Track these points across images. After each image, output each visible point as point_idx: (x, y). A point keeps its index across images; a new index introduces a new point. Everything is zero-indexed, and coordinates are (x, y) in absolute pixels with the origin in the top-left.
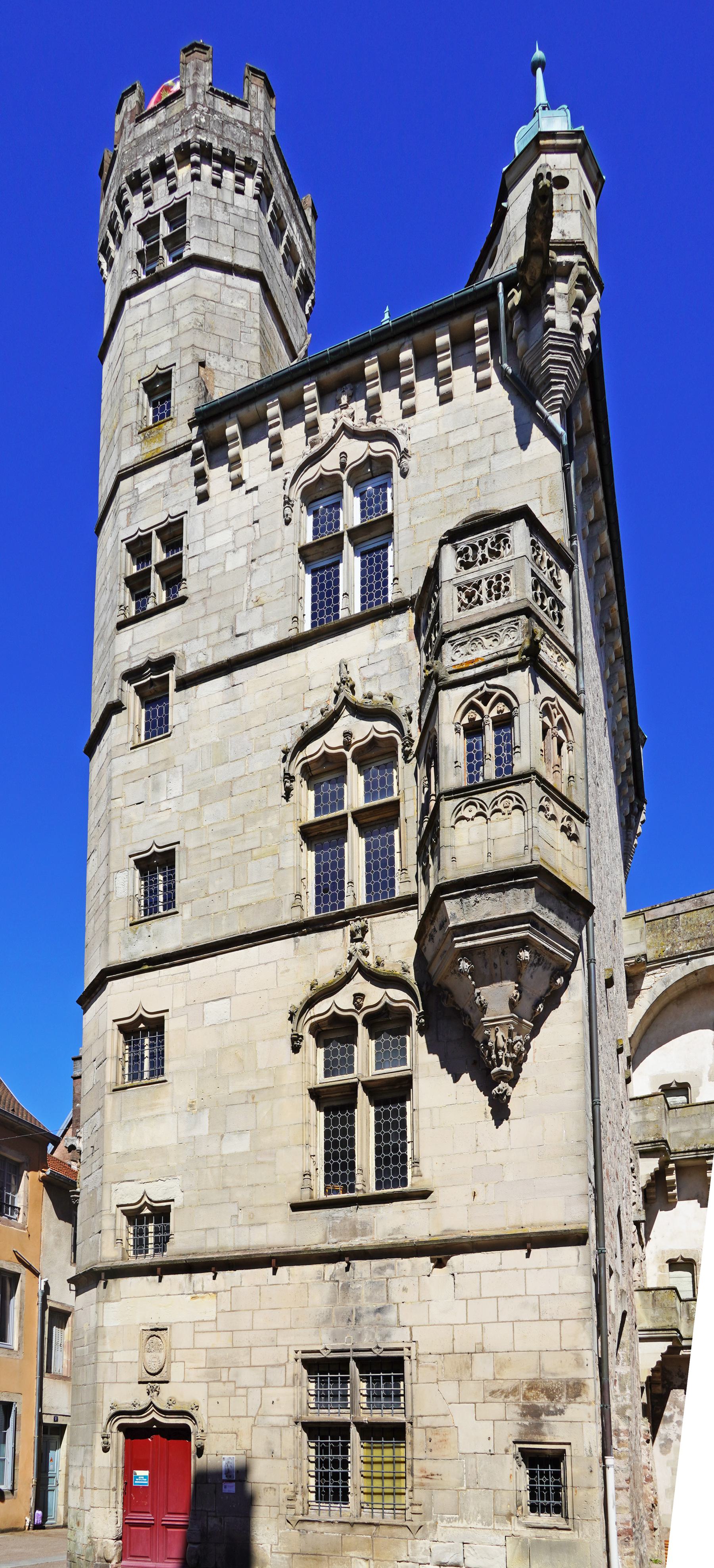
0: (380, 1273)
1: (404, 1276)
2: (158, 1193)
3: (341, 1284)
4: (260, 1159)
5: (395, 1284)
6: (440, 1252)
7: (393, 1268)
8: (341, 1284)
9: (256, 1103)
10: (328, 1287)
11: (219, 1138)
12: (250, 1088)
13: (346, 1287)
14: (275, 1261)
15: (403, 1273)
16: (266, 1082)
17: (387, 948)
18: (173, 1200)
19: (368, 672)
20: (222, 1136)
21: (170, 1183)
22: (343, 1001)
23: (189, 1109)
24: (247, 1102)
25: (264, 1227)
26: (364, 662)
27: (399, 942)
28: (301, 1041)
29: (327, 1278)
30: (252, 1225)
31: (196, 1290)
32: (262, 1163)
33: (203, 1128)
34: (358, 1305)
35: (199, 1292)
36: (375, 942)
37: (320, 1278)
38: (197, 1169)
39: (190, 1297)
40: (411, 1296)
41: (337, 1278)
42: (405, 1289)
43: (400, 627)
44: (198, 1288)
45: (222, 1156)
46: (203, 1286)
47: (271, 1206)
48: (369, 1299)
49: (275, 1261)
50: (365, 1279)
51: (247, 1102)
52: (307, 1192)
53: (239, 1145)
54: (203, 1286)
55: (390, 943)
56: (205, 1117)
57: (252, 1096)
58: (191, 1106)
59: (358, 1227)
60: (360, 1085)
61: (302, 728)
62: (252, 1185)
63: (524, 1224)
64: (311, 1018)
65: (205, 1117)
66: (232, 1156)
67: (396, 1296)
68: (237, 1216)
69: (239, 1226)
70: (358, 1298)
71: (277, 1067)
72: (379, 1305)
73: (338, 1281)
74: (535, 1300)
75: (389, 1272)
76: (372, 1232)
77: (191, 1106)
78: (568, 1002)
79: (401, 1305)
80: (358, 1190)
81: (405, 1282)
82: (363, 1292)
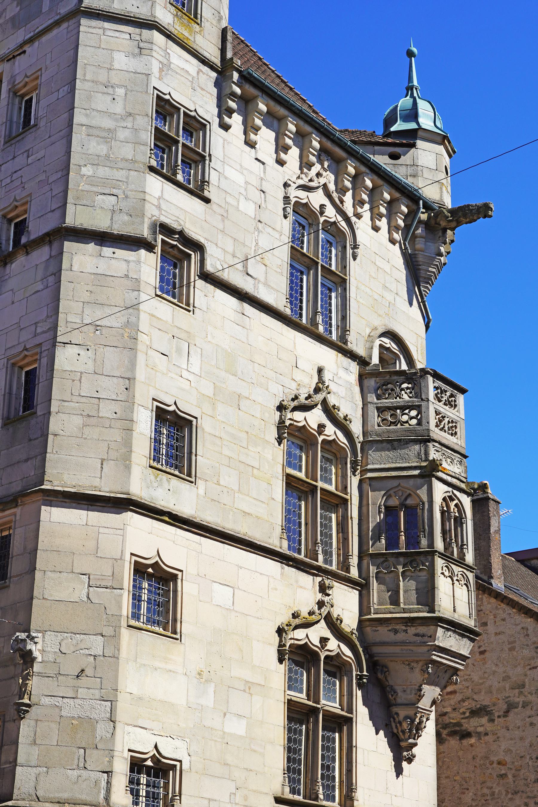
2: (170, 750)
11: (222, 715)
12: (247, 679)
20: (225, 714)
21: (178, 743)
23: (198, 677)
32: (255, 751)
33: (209, 700)
38: (203, 738)
43: (351, 369)
45: (224, 733)
47: (261, 793)
58: (199, 674)
62: (247, 769)
68: (235, 794)
71: (267, 669)
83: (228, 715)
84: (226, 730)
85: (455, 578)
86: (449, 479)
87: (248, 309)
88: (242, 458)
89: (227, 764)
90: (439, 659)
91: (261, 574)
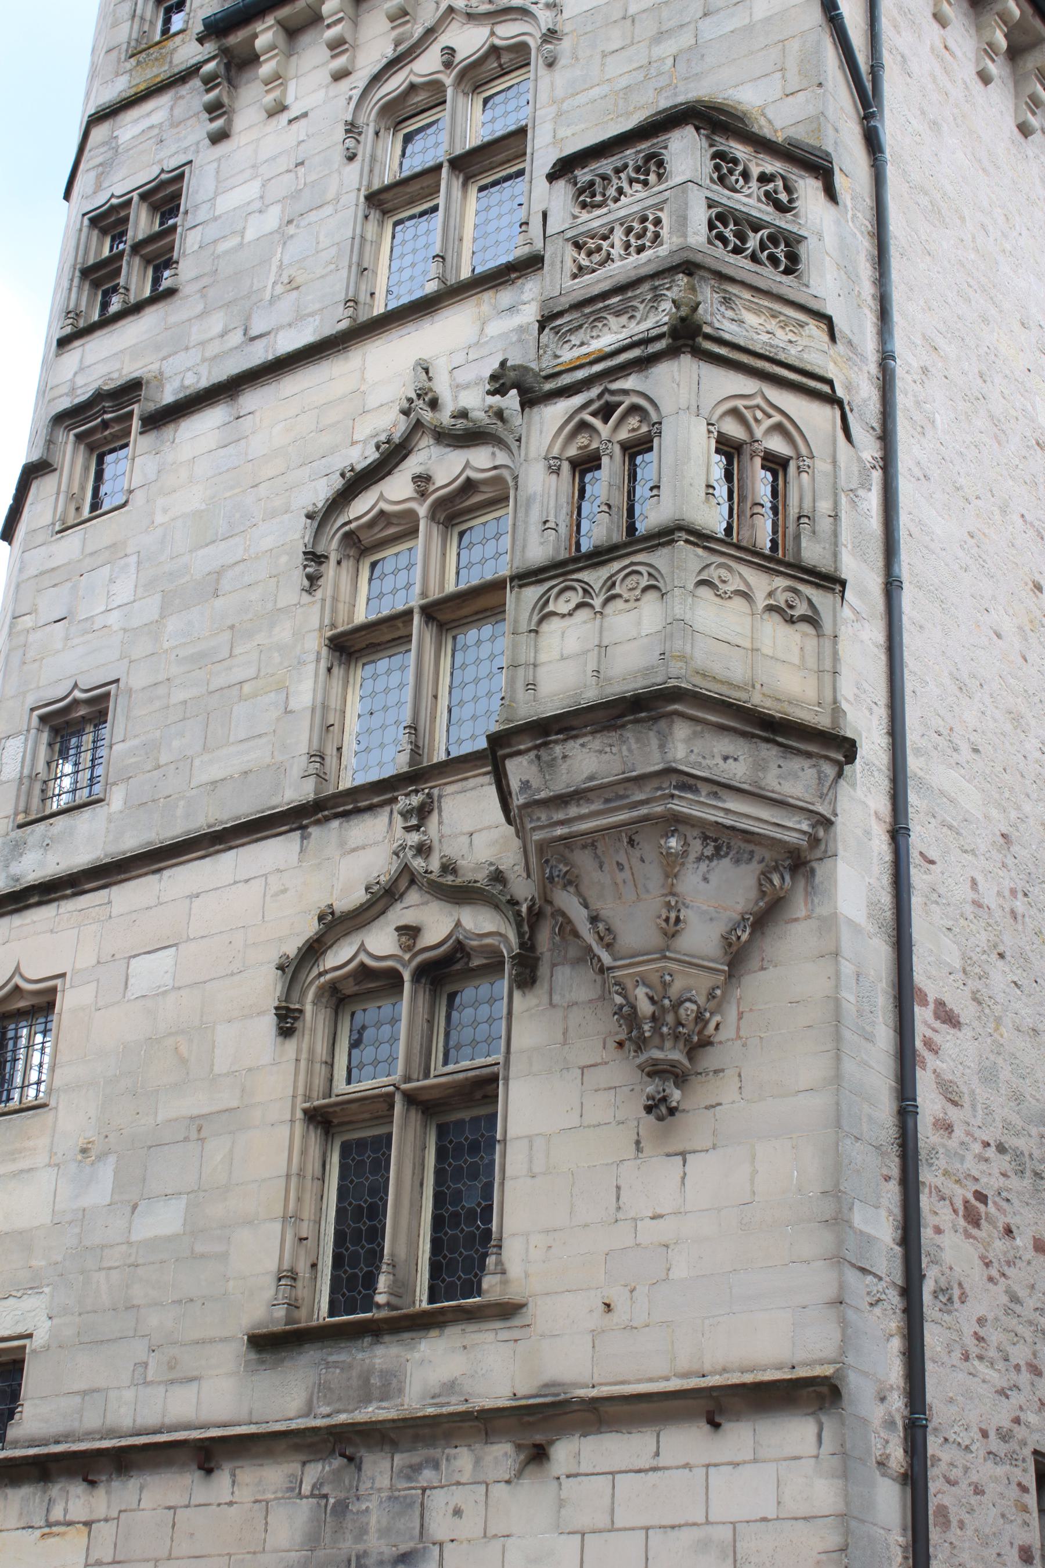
0: (409, 1478)
1: (458, 1483)
3: (332, 1501)
4: (199, 1248)
5: (440, 1502)
6: (536, 1427)
7: (436, 1466)
8: (332, 1501)
9: (202, 1140)
10: (305, 1508)
11: (129, 1209)
12: (196, 1112)
13: (341, 1509)
14: (208, 1454)
15: (457, 1477)
16: (228, 1099)
17: (465, 839)
18: (30, 1336)
19: (462, 377)
20: (135, 1207)
22: (380, 942)
23: (79, 1157)
24: (186, 1139)
25: (195, 1385)
26: (459, 359)
27: (489, 828)
28: (296, 1019)
29: (306, 1489)
30: (172, 1382)
31: (53, 1518)
32: (202, 1256)
34: (360, 1547)
35: (58, 1523)
36: (446, 830)
37: (292, 1489)
38: (82, 1273)
39: (38, 1533)
40: (470, 1526)
41: (325, 1490)
42: (457, 1512)
44: (57, 1514)
46: (66, 1511)
47: (212, 1341)
48: (384, 1532)
49: (208, 1454)
50: (380, 1490)
51: (186, 1139)
52: (280, 1312)
53: (163, 1220)
54: (66, 1511)
55: (471, 829)
56: (106, 1173)
57: (199, 1127)
59: (375, 1380)
60: (398, 1098)
61: (343, 475)
62: (180, 1302)
63: (707, 1367)
64: (320, 974)
65: (106, 1173)
66: (153, 1244)
67: (440, 1526)
68: (145, 1365)
69: (146, 1383)
70: (362, 1532)
71: (250, 1070)
72: (404, 1548)
73: (325, 1496)
74: (726, 1533)
75: (428, 1475)
76: (401, 1391)
77: (84, 1151)
78: (808, 917)
79: (448, 1547)
80: (379, 1306)
81: (458, 1496)
82: (373, 1520)
83: (142, 1205)
84: (134, 1238)
85: (597, 602)
86: (580, 375)
87: (252, 399)
88: (218, 682)
89: (133, 1306)
90: (559, 831)
91: (247, 881)
